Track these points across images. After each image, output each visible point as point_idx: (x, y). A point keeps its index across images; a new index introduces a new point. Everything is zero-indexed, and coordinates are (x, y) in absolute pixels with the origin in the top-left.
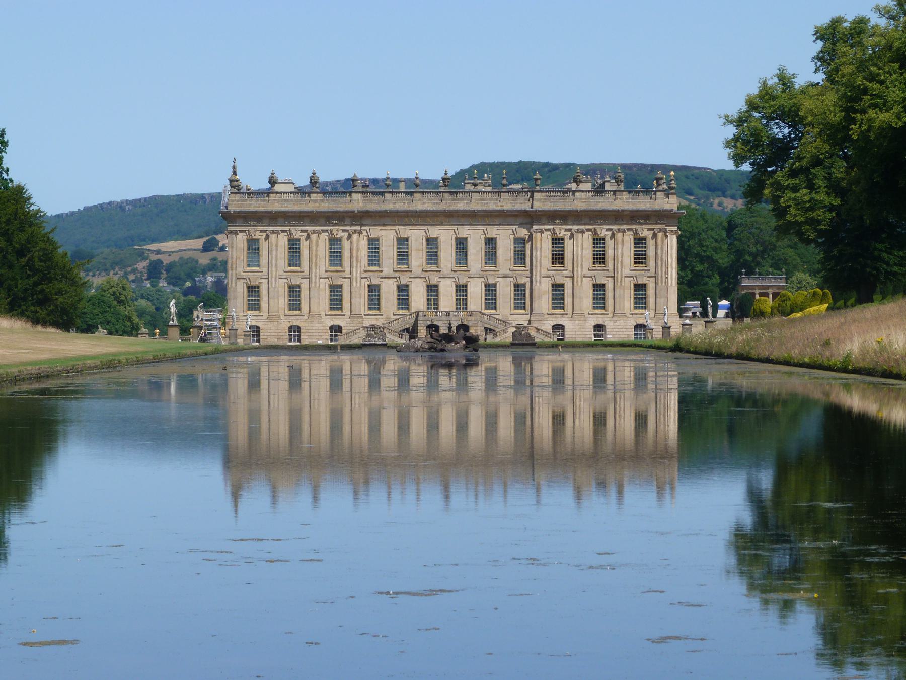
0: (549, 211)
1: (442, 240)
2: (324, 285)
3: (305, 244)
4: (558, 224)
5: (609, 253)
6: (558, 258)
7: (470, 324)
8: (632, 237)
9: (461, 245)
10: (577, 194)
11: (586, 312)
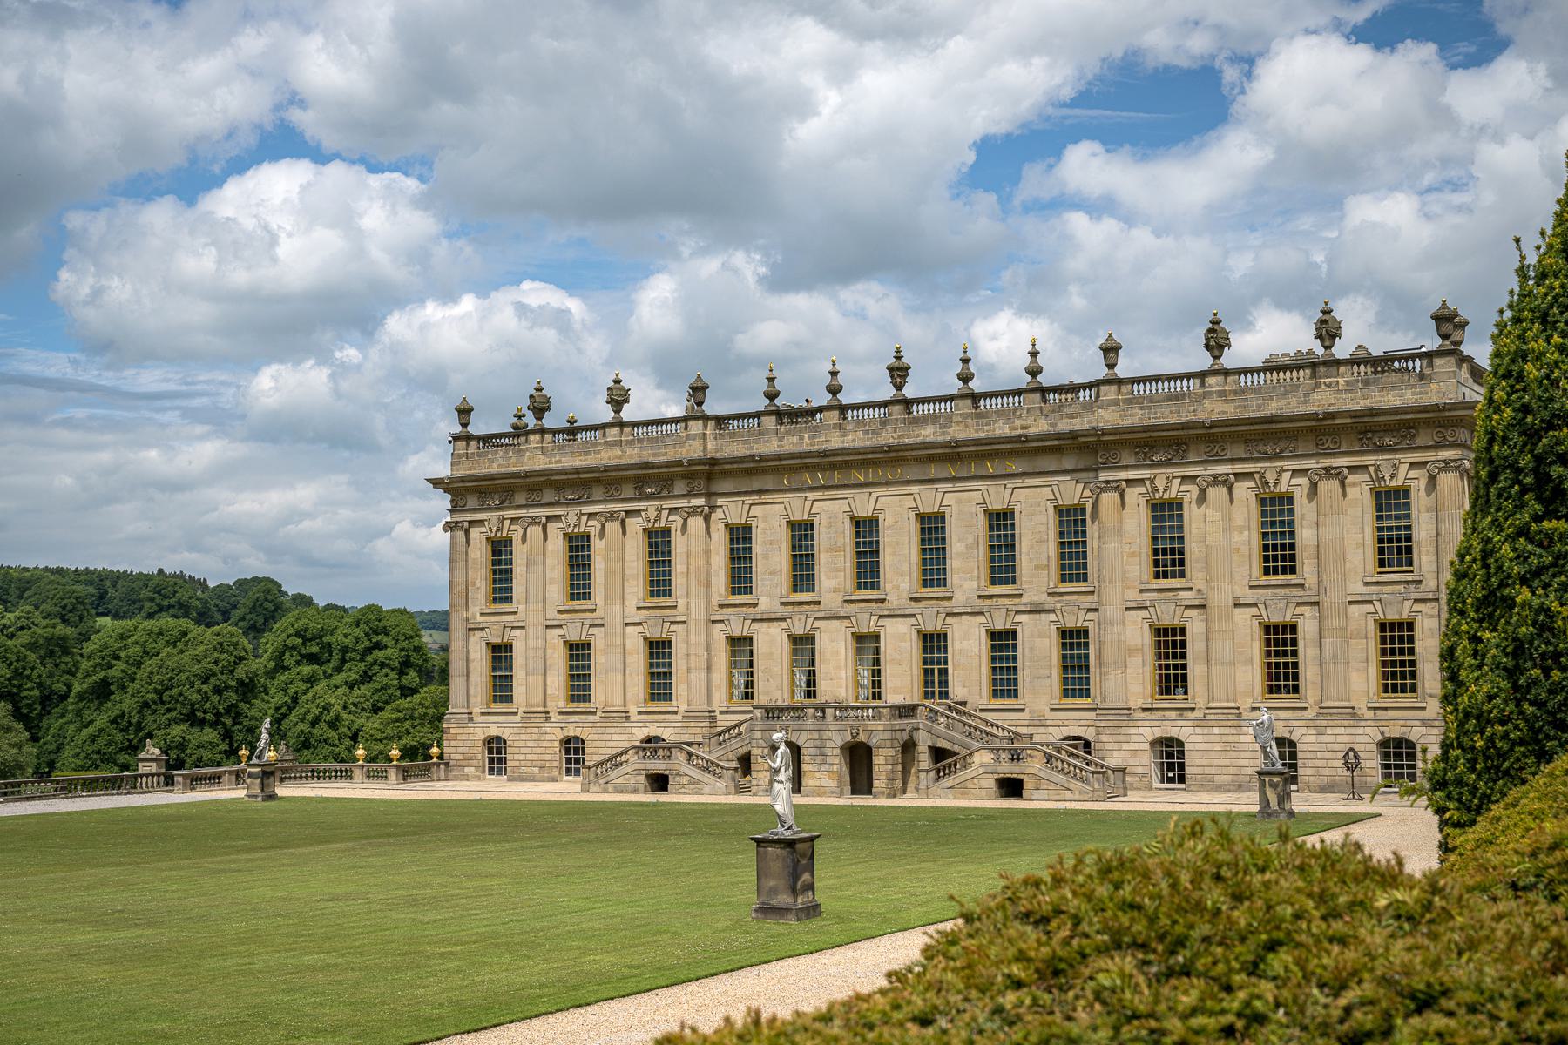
0: (1131, 430)
1: (886, 520)
2: (635, 642)
3: (597, 545)
4: (1159, 465)
5: (1305, 536)
6: (1168, 558)
7: (873, 742)
8: (1366, 488)
9: (932, 527)
10: (1211, 380)
11: (1246, 703)
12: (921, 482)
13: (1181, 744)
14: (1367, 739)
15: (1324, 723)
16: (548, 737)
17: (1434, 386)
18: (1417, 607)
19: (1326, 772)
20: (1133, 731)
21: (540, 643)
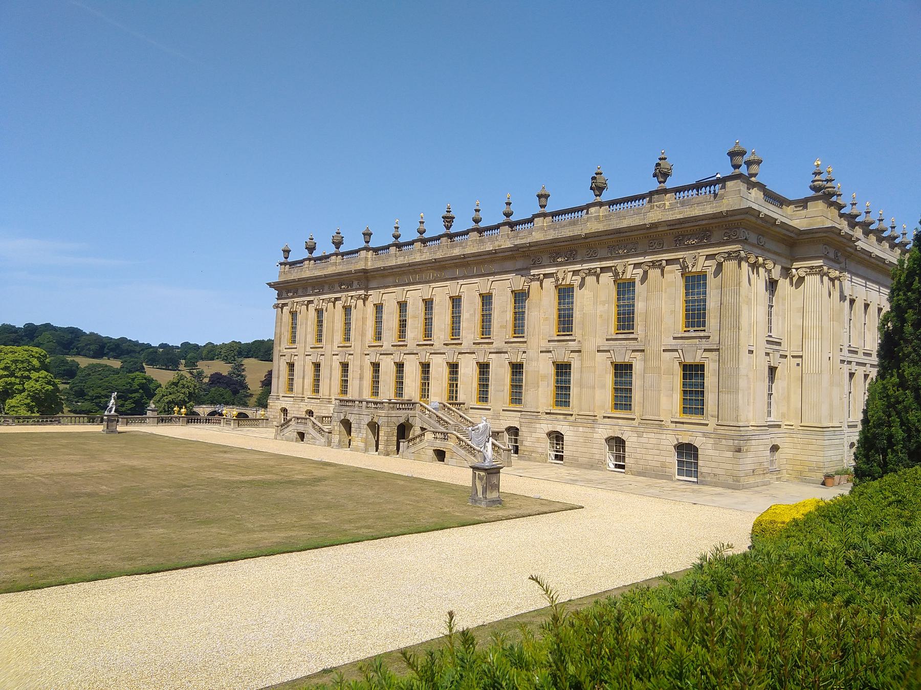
6: (565, 322)
11: (600, 414)
18: (706, 354)
19: (642, 462)
20: (538, 426)
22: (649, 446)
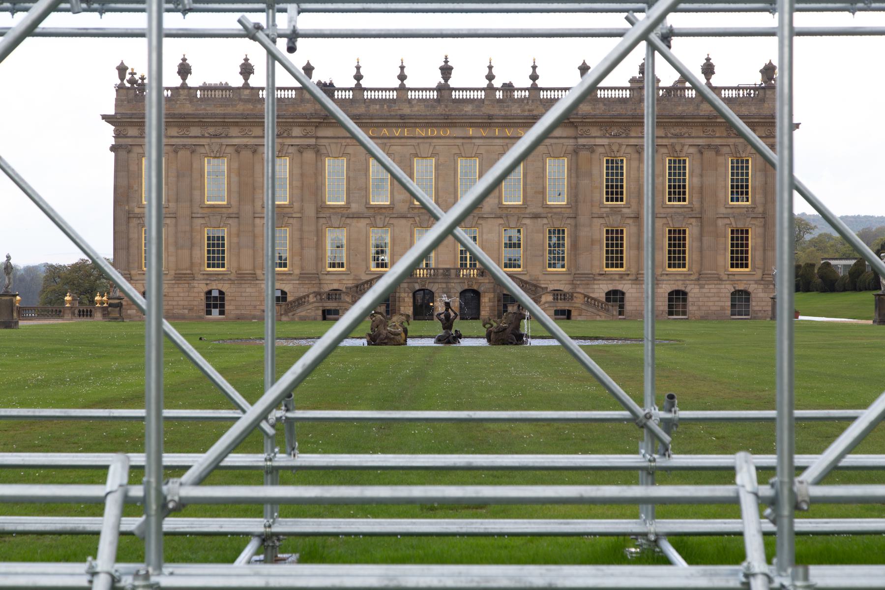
4: (615, 136)
6: (614, 192)
12: (463, 138)
13: (623, 294)
14: (726, 291)
15: (704, 282)
16: (196, 290)
17: (766, 105)
19: (704, 308)
20: (596, 286)
21: (188, 228)
22: (710, 295)
